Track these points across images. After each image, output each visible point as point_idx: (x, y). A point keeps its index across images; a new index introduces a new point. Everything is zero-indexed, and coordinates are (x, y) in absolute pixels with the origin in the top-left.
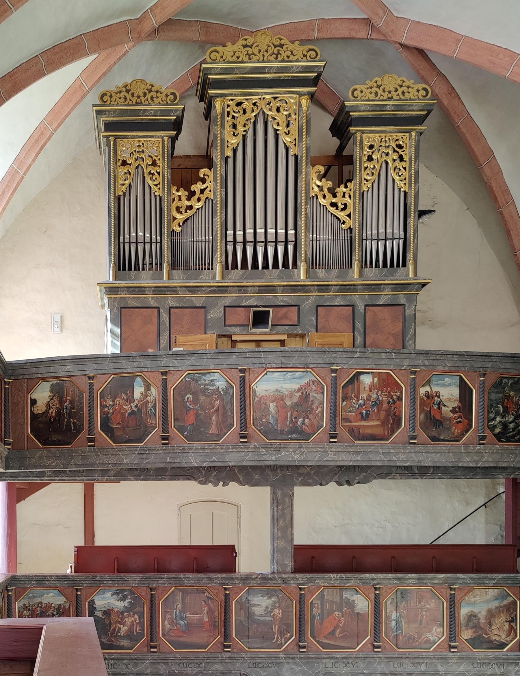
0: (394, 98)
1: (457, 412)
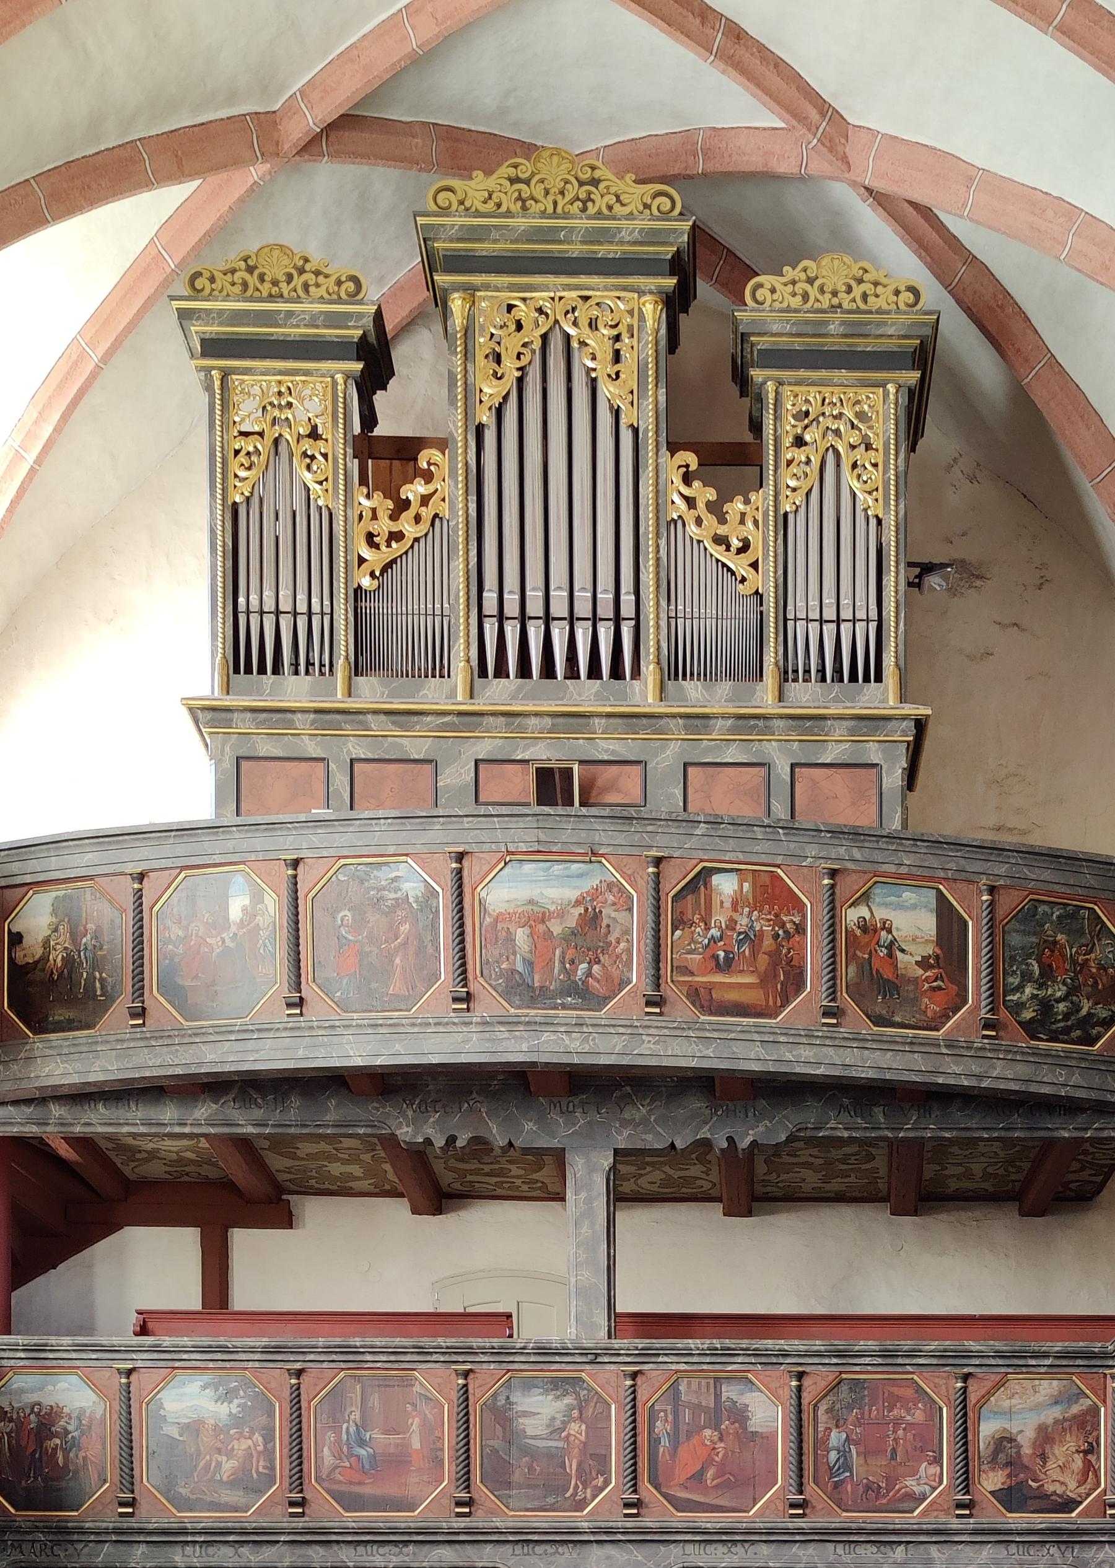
0: (845, 305)
1: (932, 967)
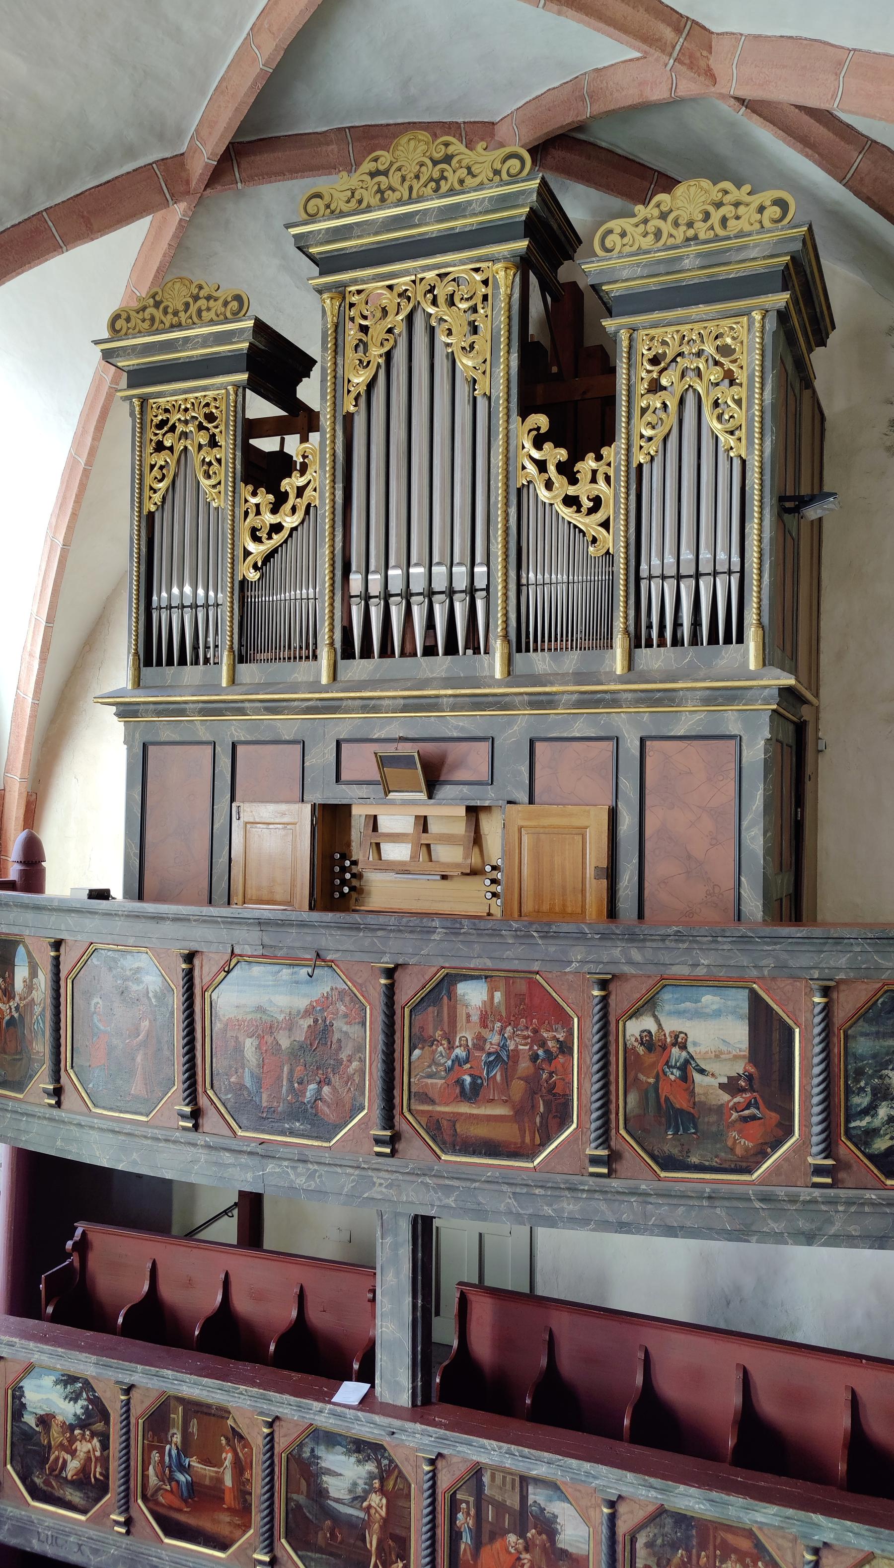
1: (742, 1090)
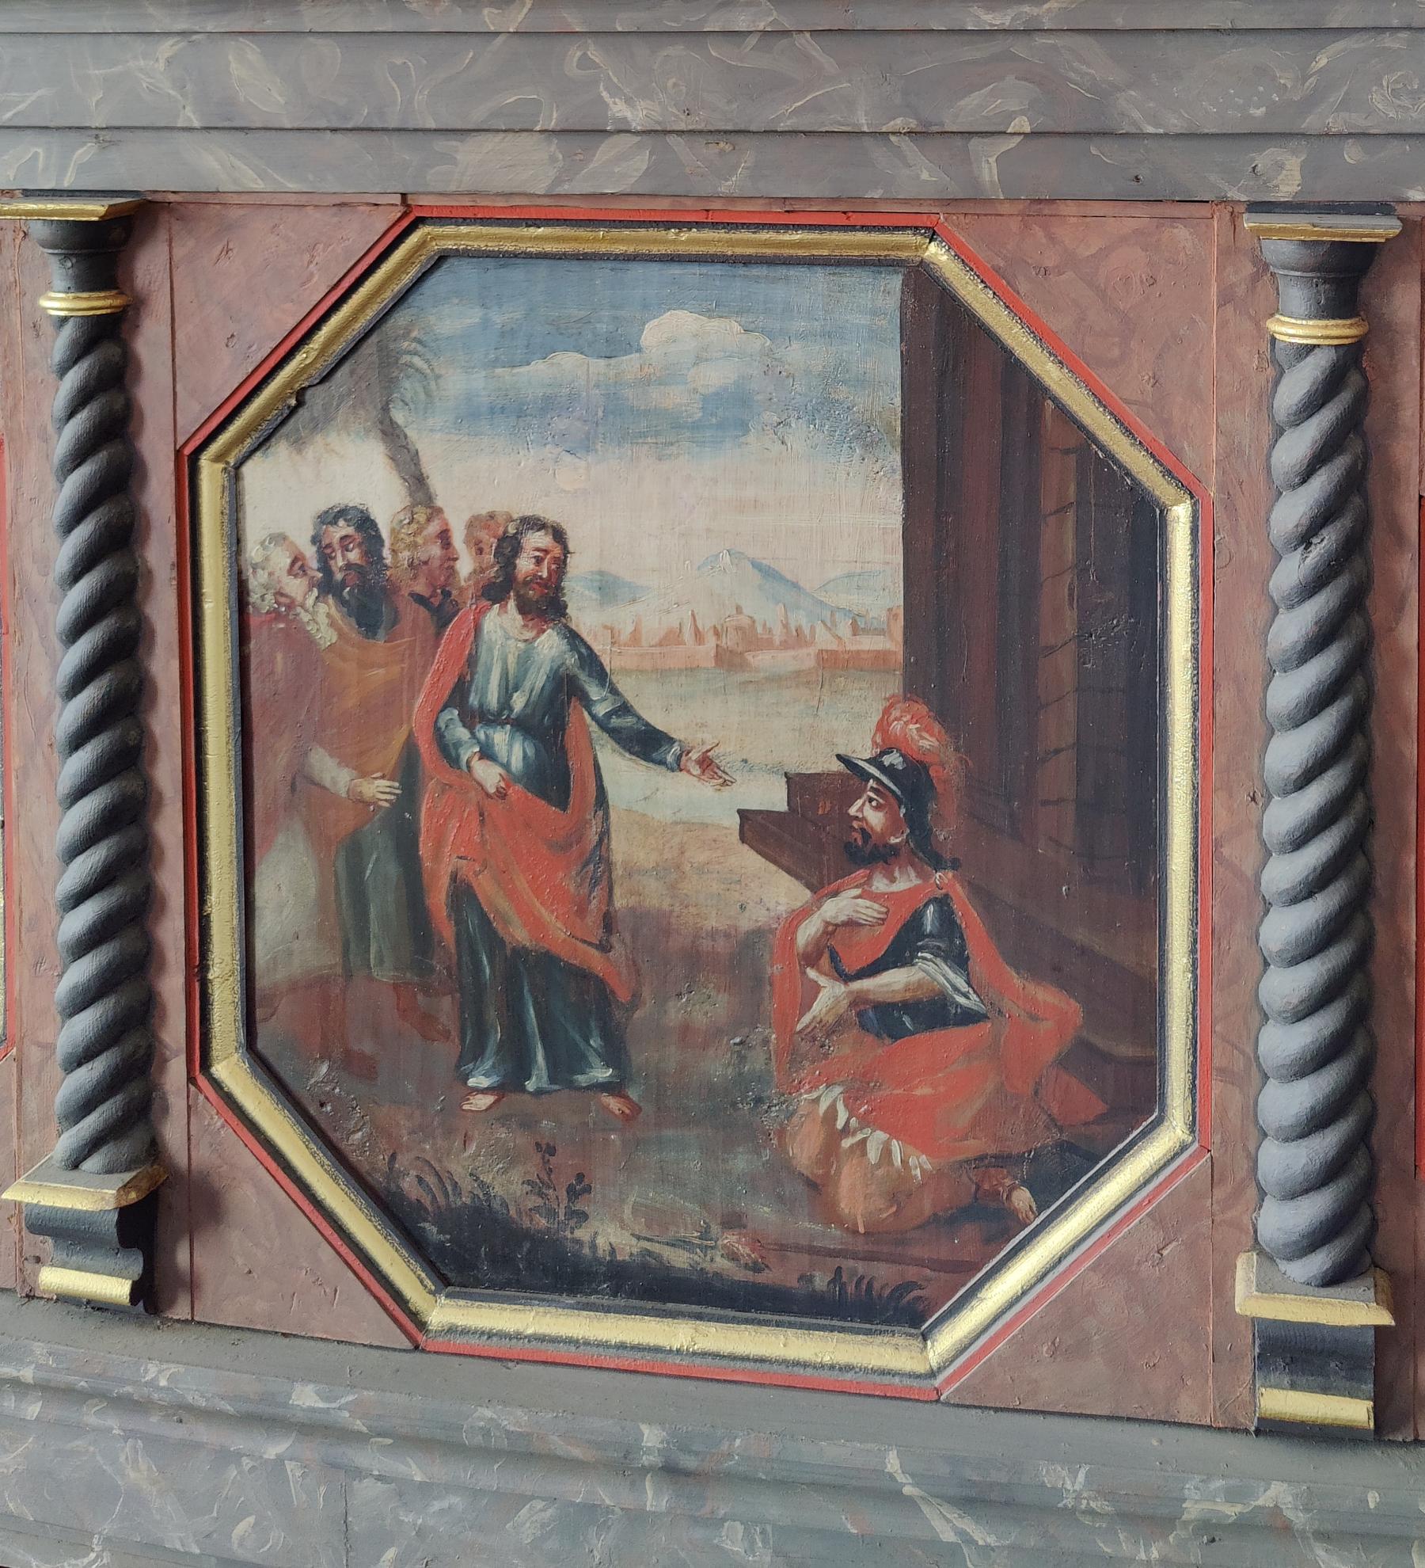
1: (868, 854)
